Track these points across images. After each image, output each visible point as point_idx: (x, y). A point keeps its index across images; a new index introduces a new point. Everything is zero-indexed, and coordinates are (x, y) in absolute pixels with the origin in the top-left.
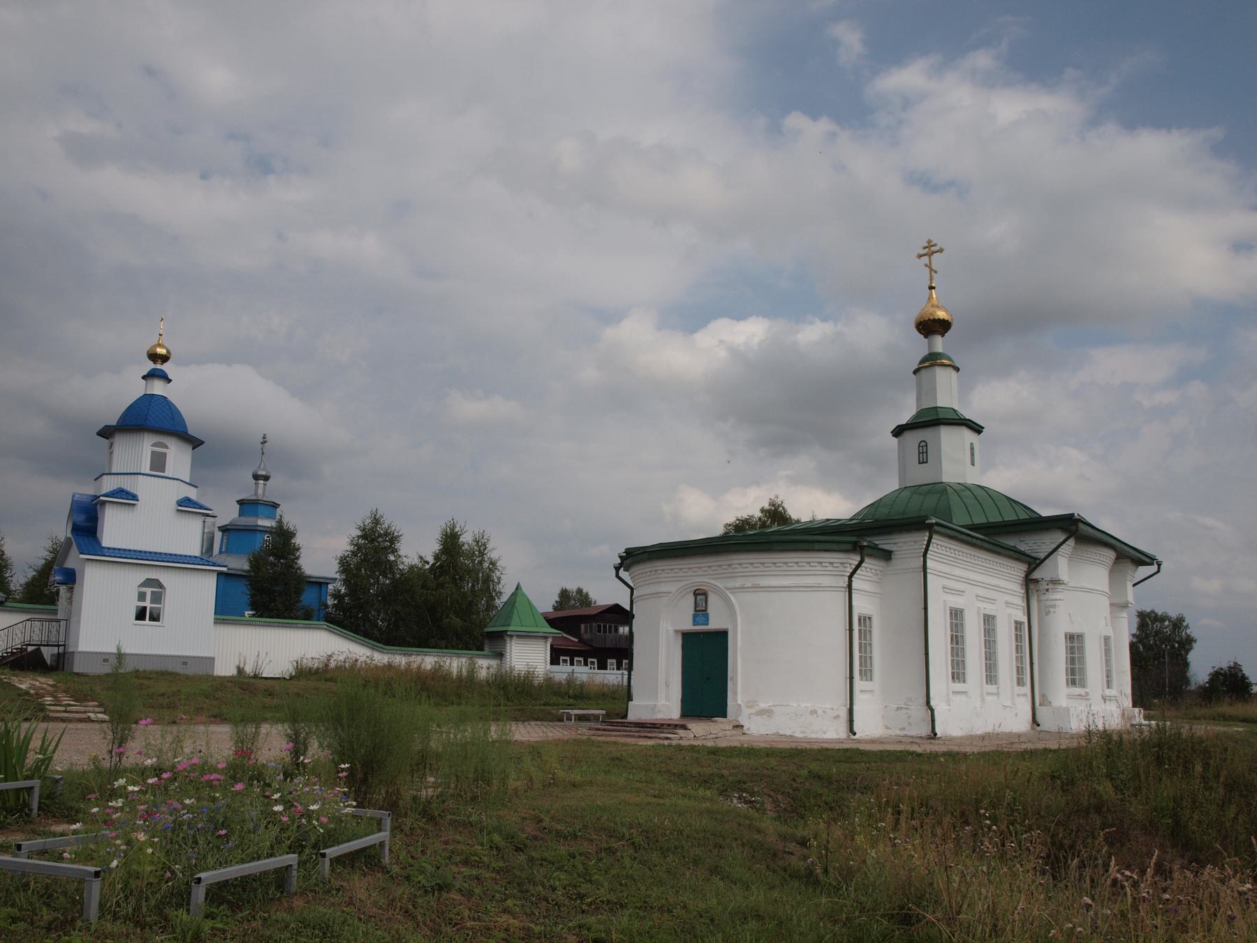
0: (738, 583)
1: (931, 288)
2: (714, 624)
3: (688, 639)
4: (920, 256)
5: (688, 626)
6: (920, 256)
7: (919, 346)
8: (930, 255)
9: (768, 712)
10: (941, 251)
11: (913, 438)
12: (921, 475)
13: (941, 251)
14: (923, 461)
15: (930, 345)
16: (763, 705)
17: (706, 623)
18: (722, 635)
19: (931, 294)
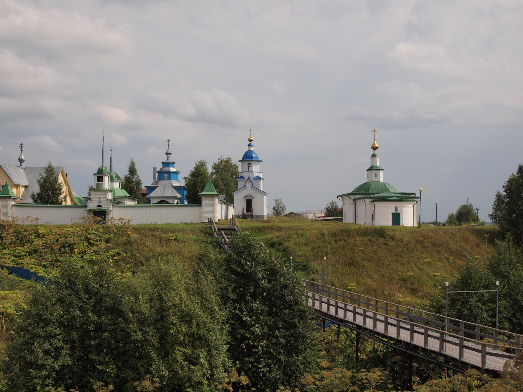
0: (403, 206)
1: (375, 139)
2: (398, 212)
3: (393, 214)
4: (372, 132)
5: (394, 212)
6: (372, 132)
7: (372, 152)
8: (375, 132)
9: (406, 224)
10: (377, 132)
11: (374, 172)
12: (374, 179)
13: (377, 132)
14: (376, 177)
15: (374, 152)
16: (407, 223)
17: (397, 211)
18: (399, 213)
19: (374, 142)
